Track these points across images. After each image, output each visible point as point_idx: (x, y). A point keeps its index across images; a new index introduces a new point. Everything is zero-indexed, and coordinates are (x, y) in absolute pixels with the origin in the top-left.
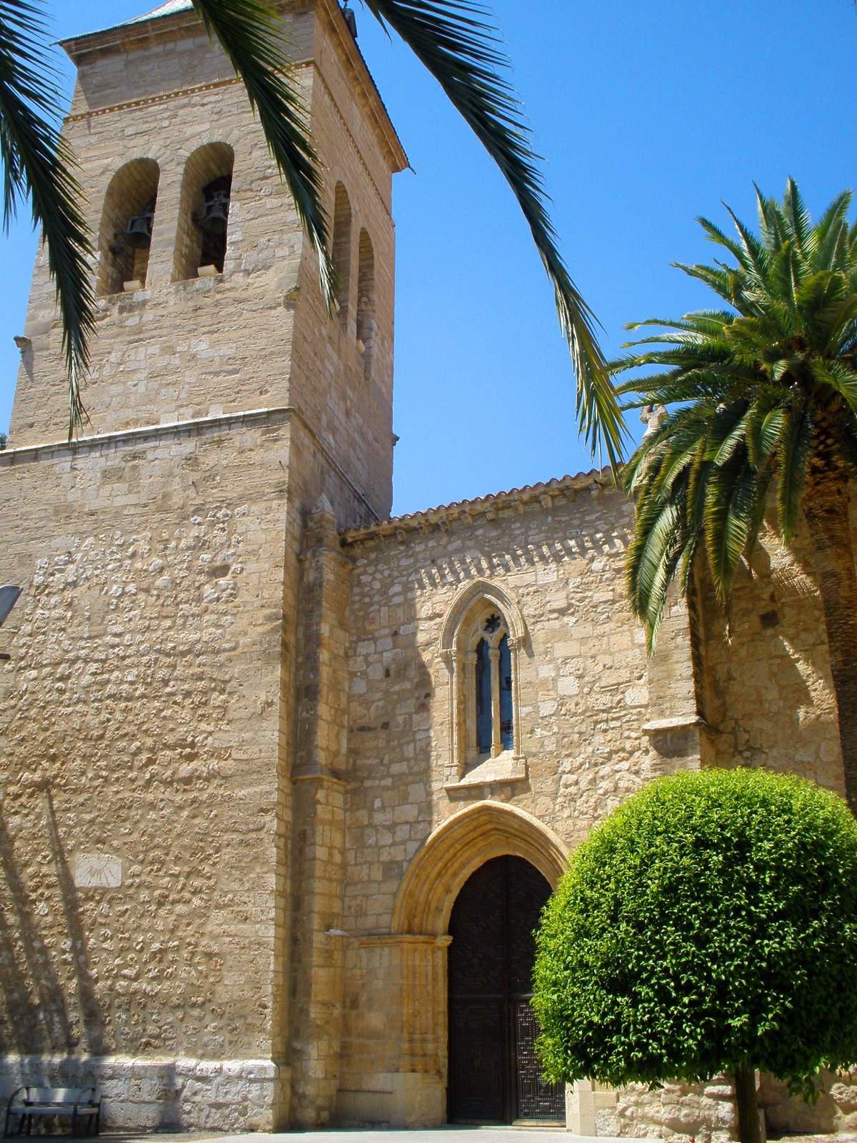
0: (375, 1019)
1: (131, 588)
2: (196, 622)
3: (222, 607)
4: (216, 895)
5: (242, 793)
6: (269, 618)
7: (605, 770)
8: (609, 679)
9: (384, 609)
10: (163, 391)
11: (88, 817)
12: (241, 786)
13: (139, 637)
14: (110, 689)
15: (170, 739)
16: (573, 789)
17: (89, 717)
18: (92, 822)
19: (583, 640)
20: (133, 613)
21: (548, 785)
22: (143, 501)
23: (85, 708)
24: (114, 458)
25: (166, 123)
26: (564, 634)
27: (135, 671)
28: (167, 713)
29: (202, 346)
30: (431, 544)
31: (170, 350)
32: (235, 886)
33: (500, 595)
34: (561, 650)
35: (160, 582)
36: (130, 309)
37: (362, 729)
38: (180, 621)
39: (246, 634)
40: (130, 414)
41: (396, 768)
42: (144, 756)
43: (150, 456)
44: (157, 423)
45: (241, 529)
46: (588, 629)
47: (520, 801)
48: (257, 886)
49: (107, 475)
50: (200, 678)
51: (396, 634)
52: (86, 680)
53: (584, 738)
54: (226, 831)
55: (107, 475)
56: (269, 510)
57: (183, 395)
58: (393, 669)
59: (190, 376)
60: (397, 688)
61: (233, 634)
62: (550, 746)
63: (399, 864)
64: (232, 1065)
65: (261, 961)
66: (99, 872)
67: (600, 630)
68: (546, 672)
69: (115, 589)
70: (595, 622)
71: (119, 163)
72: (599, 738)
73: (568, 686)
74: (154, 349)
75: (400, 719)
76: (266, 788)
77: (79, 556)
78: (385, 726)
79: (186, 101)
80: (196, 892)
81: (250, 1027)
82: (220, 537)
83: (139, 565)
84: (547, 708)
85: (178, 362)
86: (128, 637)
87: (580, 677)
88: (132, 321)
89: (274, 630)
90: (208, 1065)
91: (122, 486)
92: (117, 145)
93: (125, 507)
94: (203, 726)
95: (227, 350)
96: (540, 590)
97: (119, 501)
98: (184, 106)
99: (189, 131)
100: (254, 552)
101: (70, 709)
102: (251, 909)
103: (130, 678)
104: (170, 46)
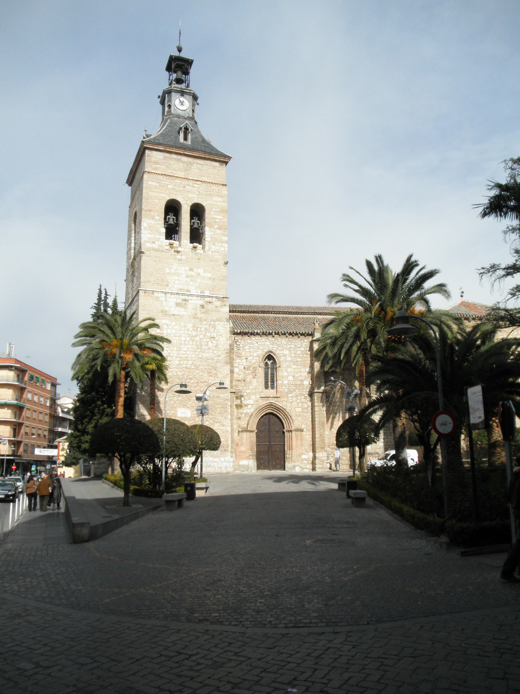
0: (243, 449)
1: (188, 339)
2: (207, 351)
3: (214, 348)
4: (216, 420)
5: (221, 395)
6: (227, 353)
7: (299, 398)
8: (300, 378)
9: (243, 352)
10: (191, 282)
11: (180, 399)
12: (221, 394)
13: (191, 353)
14: (184, 366)
15: (202, 381)
16: (291, 401)
17: (178, 373)
18: (181, 400)
19: (294, 369)
20: (188, 346)
21: (285, 399)
22: (189, 315)
23: (177, 370)
24: (179, 299)
25: (182, 189)
26: (289, 366)
27: (191, 362)
28: (201, 374)
29: (201, 271)
30: (257, 338)
31: (191, 270)
32: (221, 418)
33: (275, 354)
34: (289, 370)
35: (197, 339)
36: (178, 252)
37: (238, 381)
38: (203, 350)
39: (220, 356)
40: (180, 287)
41: (247, 391)
42: (195, 385)
43: (190, 301)
44: (190, 292)
45: (217, 328)
46: (295, 367)
47: (279, 402)
48: (226, 418)
49: (178, 304)
50: (209, 365)
51: (247, 359)
52: (177, 362)
53: (294, 390)
54: (218, 404)
55: (178, 304)
56: (224, 325)
57: (197, 285)
58: (246, 367)
59: (199, 280)
60: (247, 372)
61: (218, 356)
62: (286, 390)
63: (249, 413)
64: (222, 459)
65: (227, 435)
66: (184, 413)
67: (298, 367)
68: (285, 374)
69: (183, 339)
70: (297, 365)
71: (168, 199)
72: (297, 391)
73: (291, 378)
74: (187, 268)
75: (248, 379)
76: (227, 395)
77: (171, 327)
78: (244, 381)
79: (188, 183)
80: (211, 419)
81: (225, 450)
82: (212, 330)
83: (190, 333)
84: (286, 382)
85: (195, 274)
86: (188, 353)
87: (294, 376)
88: (179, 257)
89: (227, 356)
90: (216, 460)
91: (181, 309)
92: (166, 190)
93: (184, 315)
94: (211, 378)
95: (209, 275)
96: (285, 356)
97: (182, 313)
98: (188, 185)
99: (190, 195)
100: (221, 335)
101: (172, 370)
102: (225, 424)
103: (190, 363)
104: (179, 157)
